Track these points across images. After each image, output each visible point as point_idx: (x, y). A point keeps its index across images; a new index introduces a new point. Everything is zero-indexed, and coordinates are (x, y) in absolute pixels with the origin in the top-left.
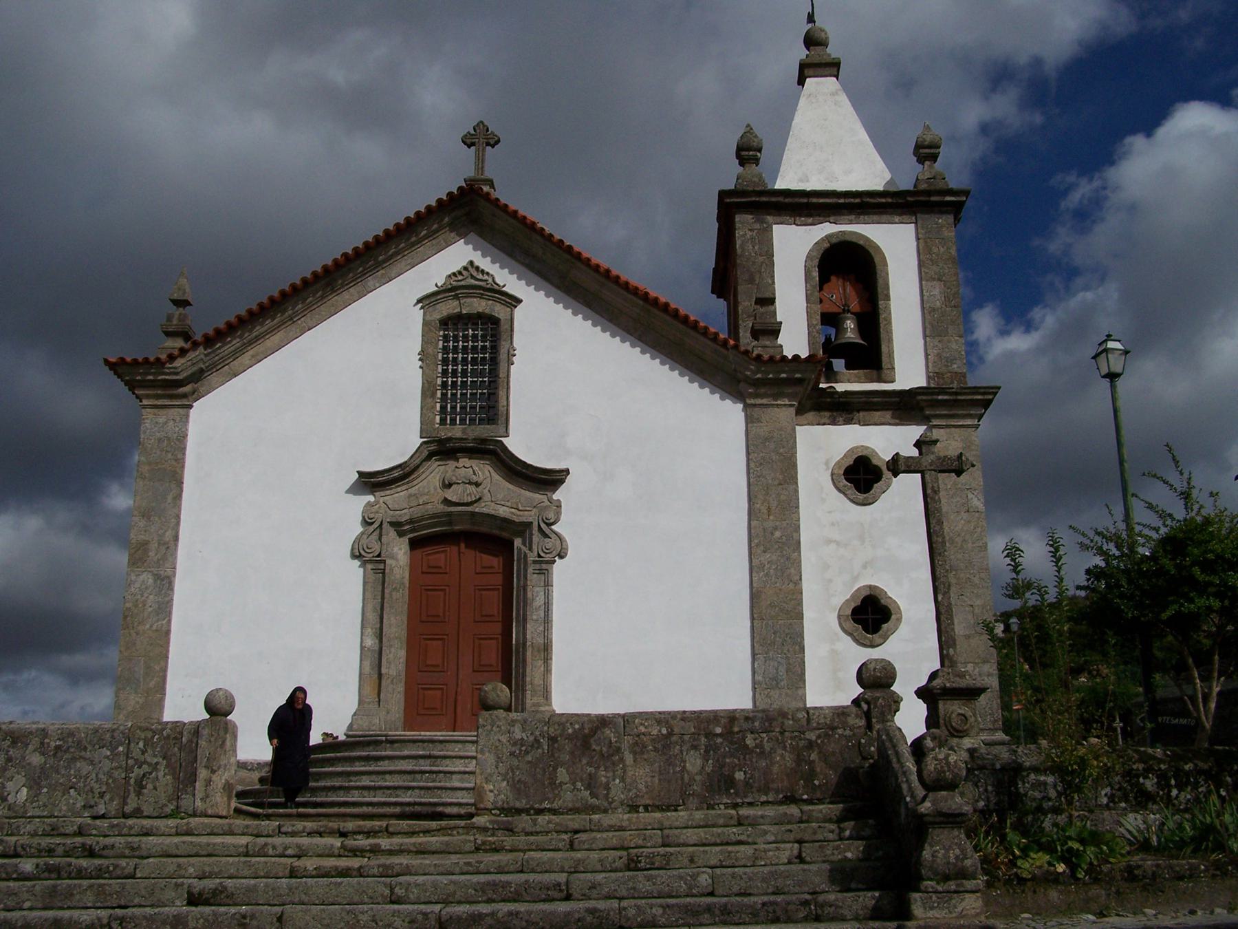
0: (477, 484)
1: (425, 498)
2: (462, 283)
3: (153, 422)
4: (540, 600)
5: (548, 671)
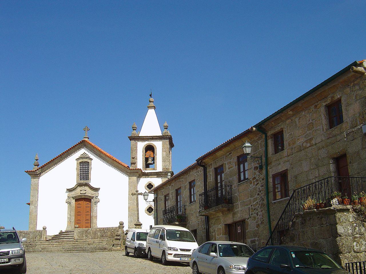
0: (86, 191)
1: (77, 193)
2: (83, 156)
3: (34, 181)
4: (95, 209)
5: (96, 220)
